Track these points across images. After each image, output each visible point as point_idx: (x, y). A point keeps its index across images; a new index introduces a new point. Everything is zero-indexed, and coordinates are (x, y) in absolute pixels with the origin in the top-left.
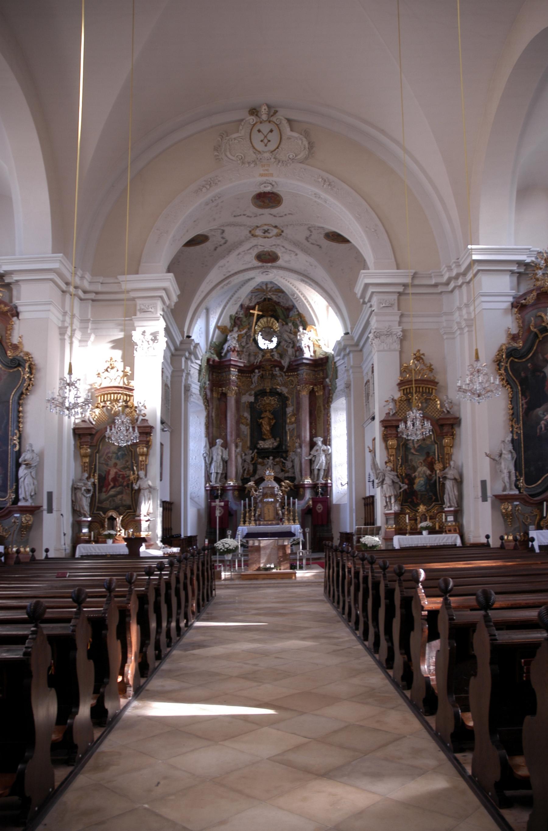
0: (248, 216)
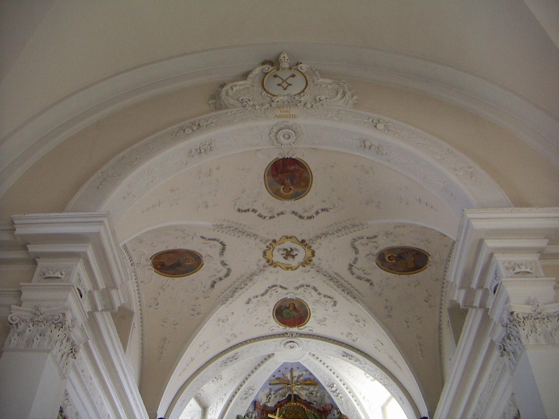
0: (260, 216)
